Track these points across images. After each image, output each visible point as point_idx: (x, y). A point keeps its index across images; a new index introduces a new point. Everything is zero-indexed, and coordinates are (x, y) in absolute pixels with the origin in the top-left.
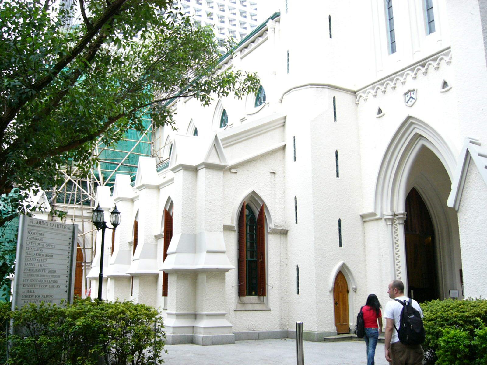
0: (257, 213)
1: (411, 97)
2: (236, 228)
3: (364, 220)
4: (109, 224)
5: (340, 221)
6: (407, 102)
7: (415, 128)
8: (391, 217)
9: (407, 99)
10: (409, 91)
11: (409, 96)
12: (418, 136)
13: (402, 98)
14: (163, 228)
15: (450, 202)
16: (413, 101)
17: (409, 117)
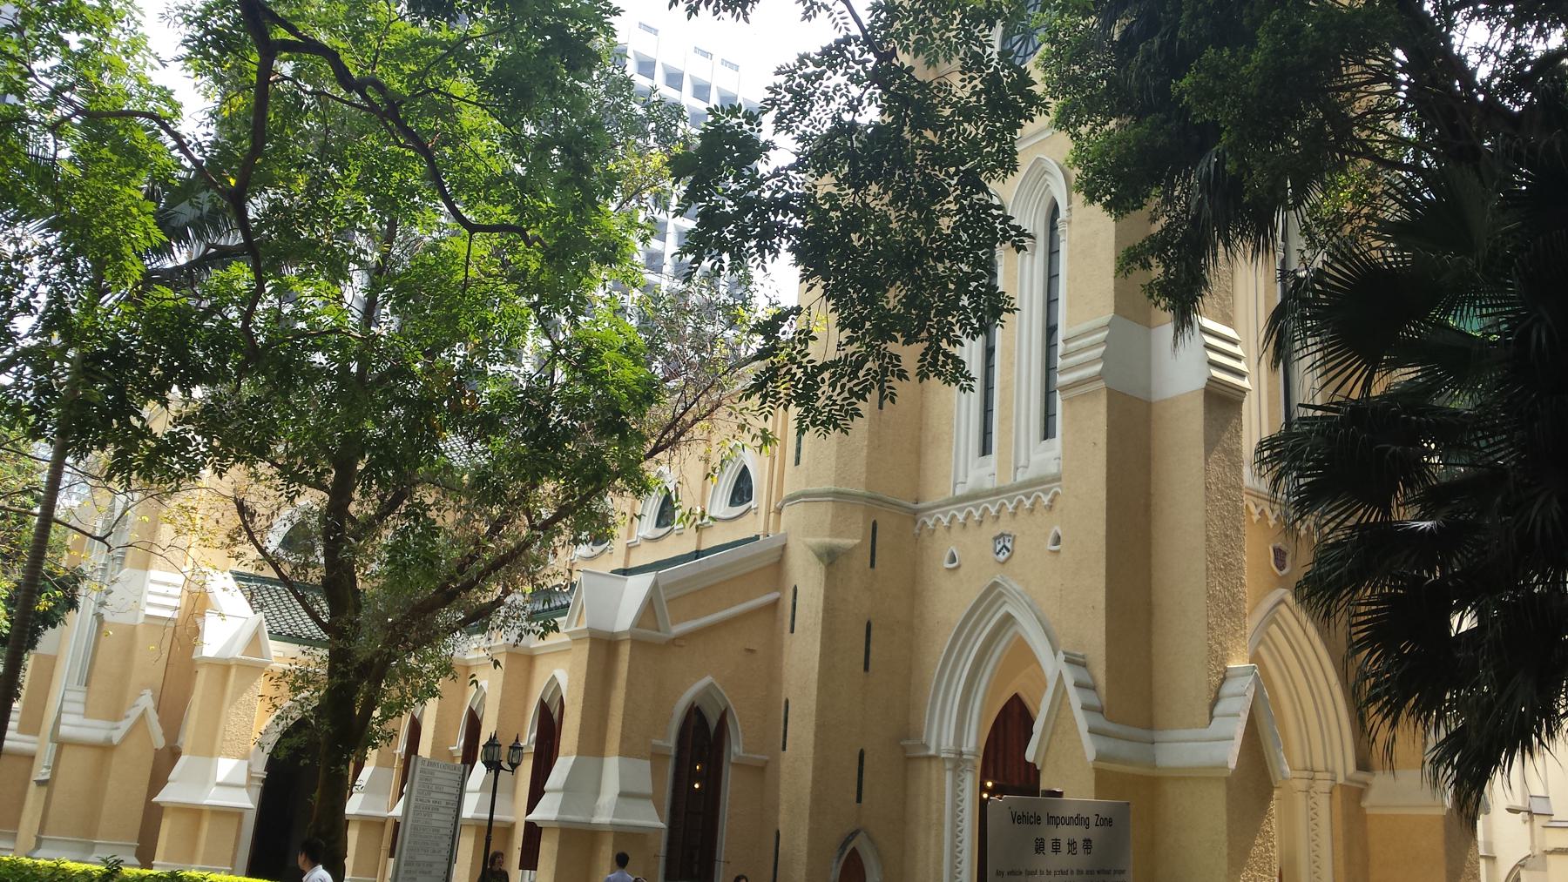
0: (713, 723)
1: (1004, 546)
2: (673, 752)
3: (908, 755)
4: (505, 764)
5: (862, 755)
6: (998, 554)
7: (1005, 602)
8: (953, 756)
9: (999, 547)
10: (1002, 535)
11: (1002, 544)
12: (1008, 619)
13: (991, 544)
14: (534, 734)
15: (1030, 755)
16: (1007, 554)
17: (995, 585)
